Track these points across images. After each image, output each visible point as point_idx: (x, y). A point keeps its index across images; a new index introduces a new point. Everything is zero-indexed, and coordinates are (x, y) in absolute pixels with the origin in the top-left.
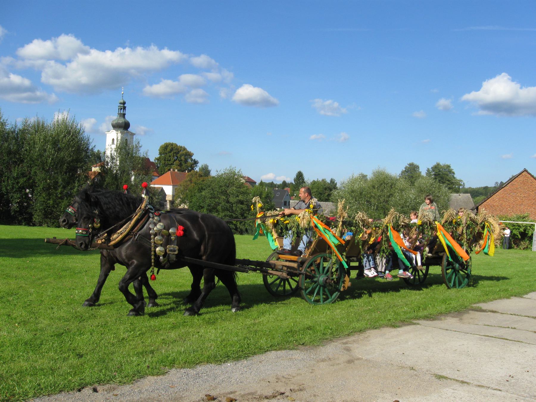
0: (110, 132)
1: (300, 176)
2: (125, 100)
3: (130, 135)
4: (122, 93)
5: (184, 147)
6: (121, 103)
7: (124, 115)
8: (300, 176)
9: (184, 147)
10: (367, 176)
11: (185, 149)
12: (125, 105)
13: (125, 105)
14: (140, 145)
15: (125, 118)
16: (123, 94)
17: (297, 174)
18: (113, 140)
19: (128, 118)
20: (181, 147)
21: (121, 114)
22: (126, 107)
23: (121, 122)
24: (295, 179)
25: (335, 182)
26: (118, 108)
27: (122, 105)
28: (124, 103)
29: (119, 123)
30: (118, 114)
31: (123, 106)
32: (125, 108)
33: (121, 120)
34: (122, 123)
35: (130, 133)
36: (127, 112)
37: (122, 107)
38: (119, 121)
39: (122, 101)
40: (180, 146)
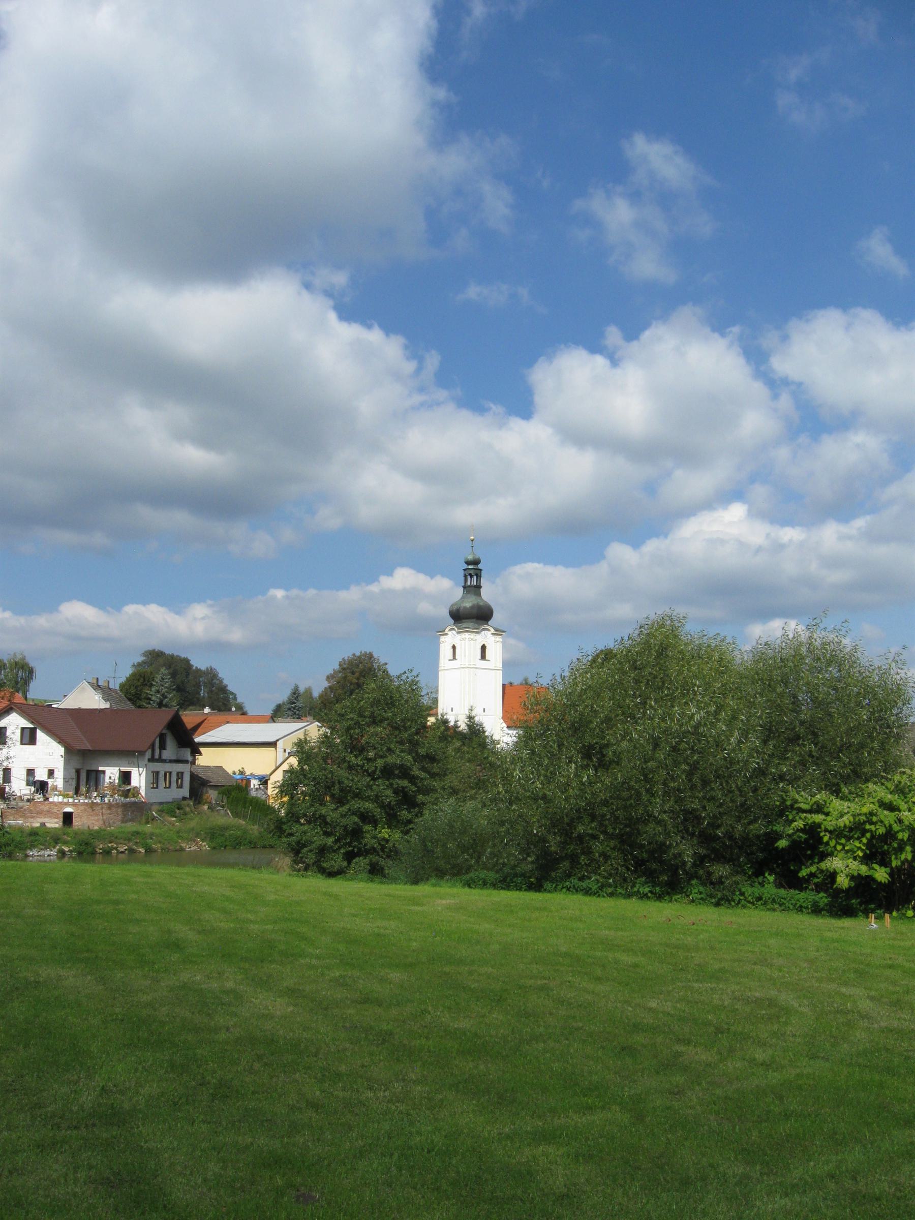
2: (479, 555)
3: (492, 634)
4: (472, 538)
6: (468, 563)
7: (479, 587)
12: (480, 566)
13: (480, 566)
15: (479, 594)
16: (472, 540)
18: (454, 647)
19: (489, 593)
21: (469, 587)
22: (481, 570)
23: (468, 604)
26: (462, 573)
27: (470, 567)
28: (476, 562)
30: (464, 587)
32: (478, 574)
33: (469, 600)
34: (472, 607)
35: (493, 631)
36: (483, 582)
39: (470, 557)
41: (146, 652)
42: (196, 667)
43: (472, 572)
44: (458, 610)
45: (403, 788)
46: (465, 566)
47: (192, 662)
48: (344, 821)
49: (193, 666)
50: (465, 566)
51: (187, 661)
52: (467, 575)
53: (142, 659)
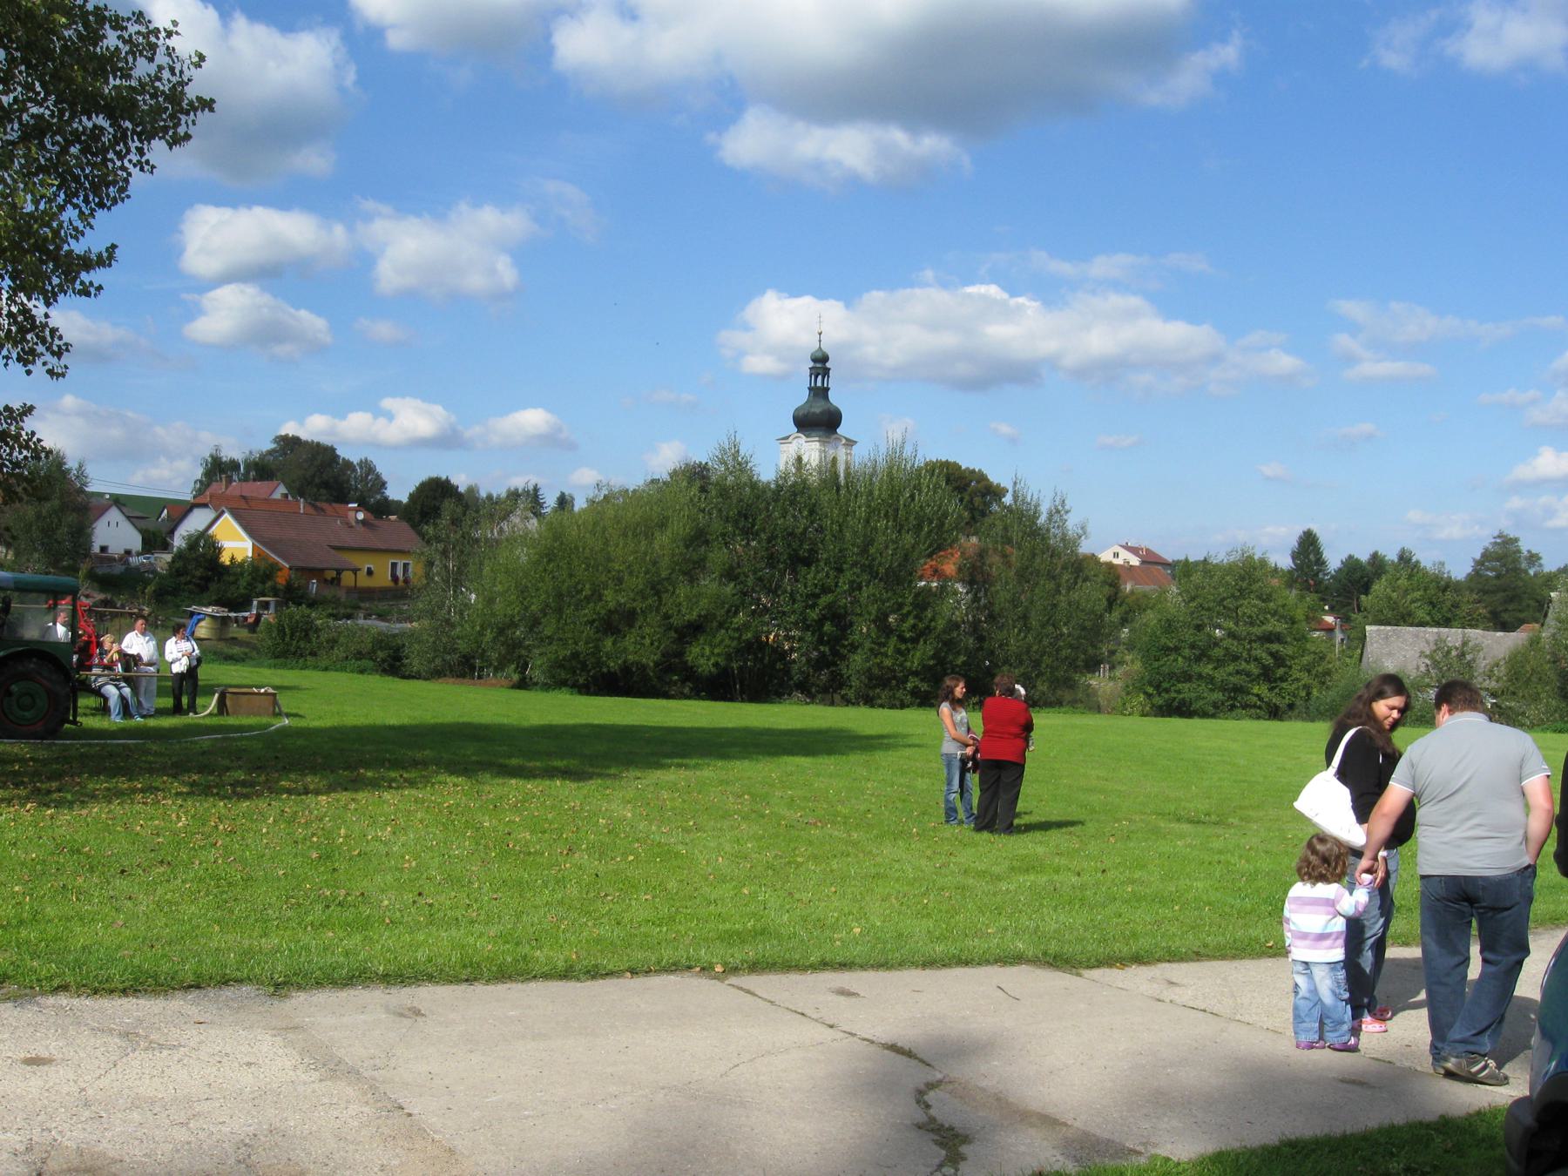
0: (790, 440)
1: (1308, 545)
5: (980, 470)
7: (828, 389)
8: (1308, 545)
9: (980, 470)
10: (1516, 540)
11: (981, 477)
12: (828, 365)
13: (828, 365)
14: (1067, 507)
15: (826, 397)
17: (1300, 537)
20: (973, 471)
23: (818, 410)
24: (1293, 552)
25: (1414, 559)
27: (819, 365)
29: (814, 413)
30: (810, 389)
31: (820, 364)
32: (826, 372)
34: (822, 413)
37: (821, 371)
38: (813, 410)
39: (819, 355)
40: (968, 468)
41: (277, 437)
42: (344, 459)
43: (821, 371)
44: (806, 416)
45: (1277, 652)
46: (811, 364)
47: (338, 452)
48: (1234, 679)
49: (339, 456)
50: (811, 364)
51: (332, 450)
52: (815, 372)
53: (273, 446)
